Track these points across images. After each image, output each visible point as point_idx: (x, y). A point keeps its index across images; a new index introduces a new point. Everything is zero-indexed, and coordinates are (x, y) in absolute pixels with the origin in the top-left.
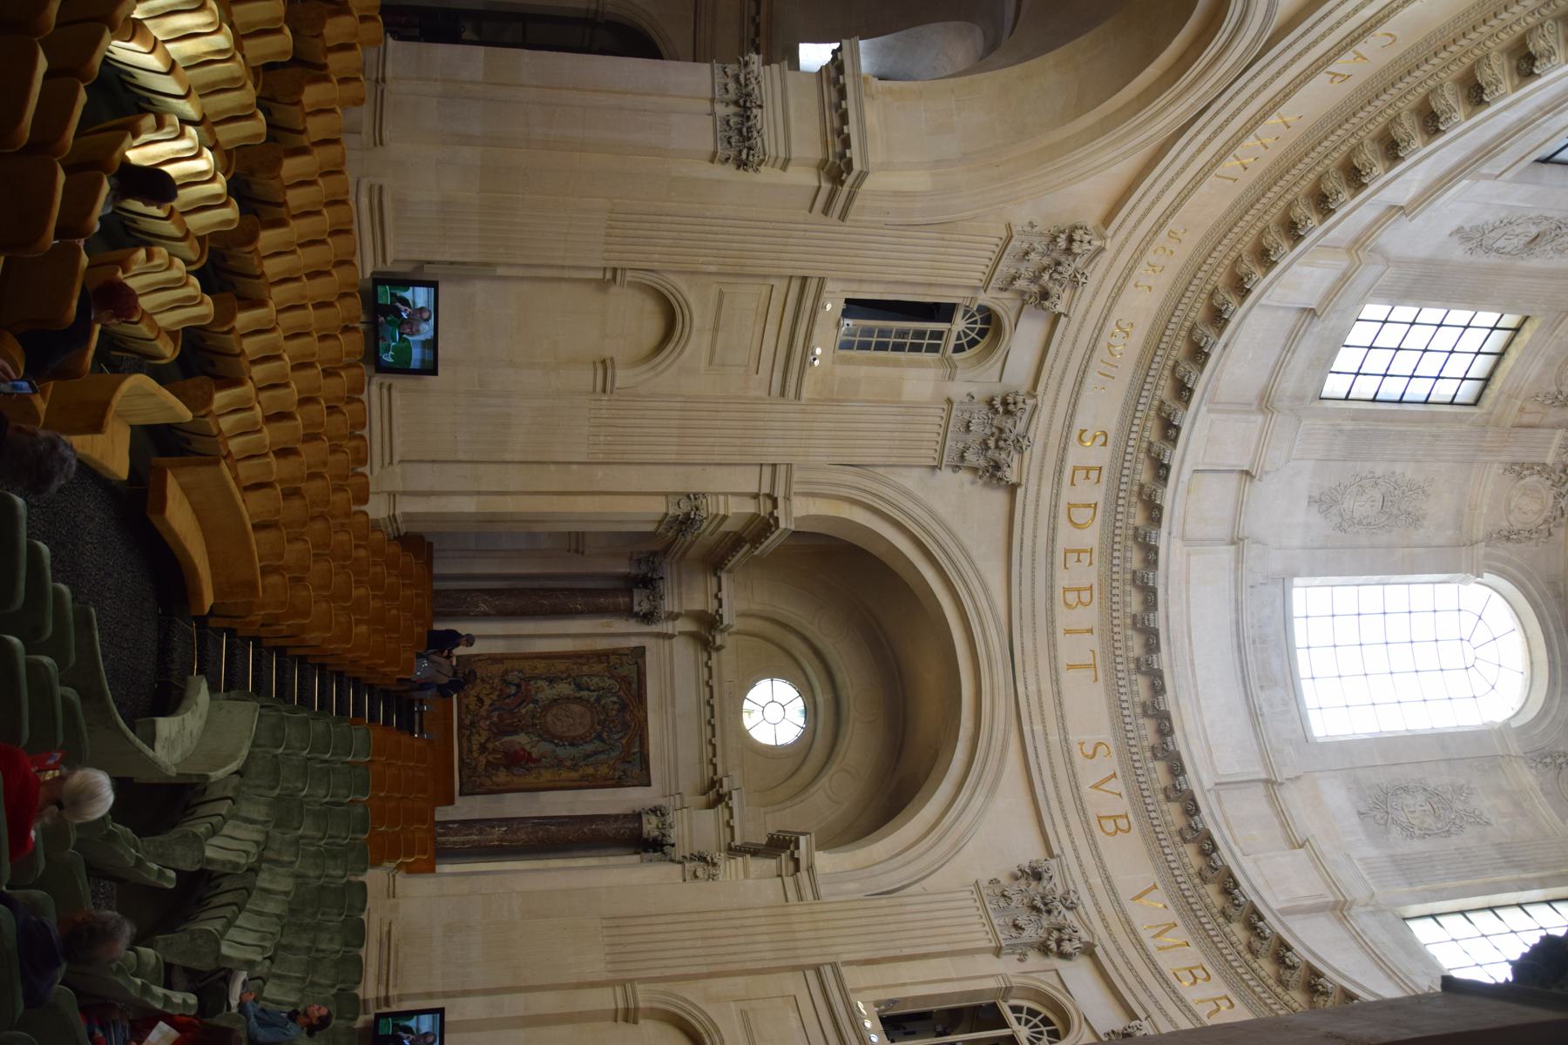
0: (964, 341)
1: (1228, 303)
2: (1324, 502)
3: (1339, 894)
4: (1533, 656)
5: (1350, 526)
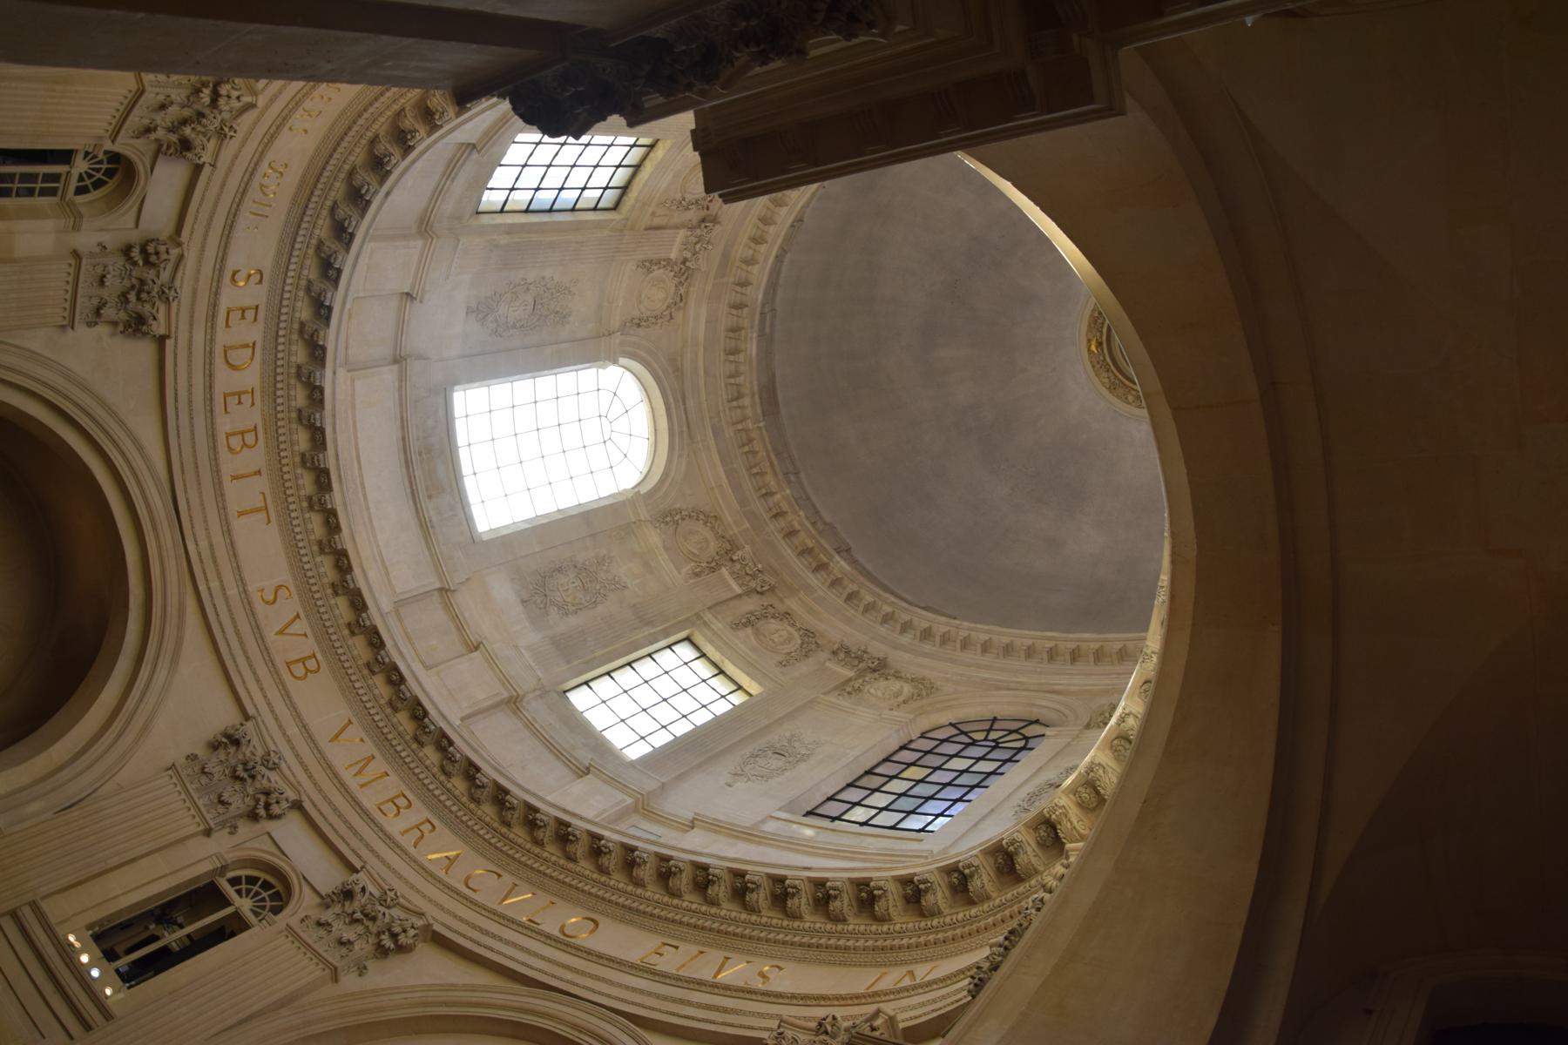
0: (88, 182)
1: (391, 155)
2: (480, 311)
3: (512, 690)
4: (657, 424)
5: (505, 330)
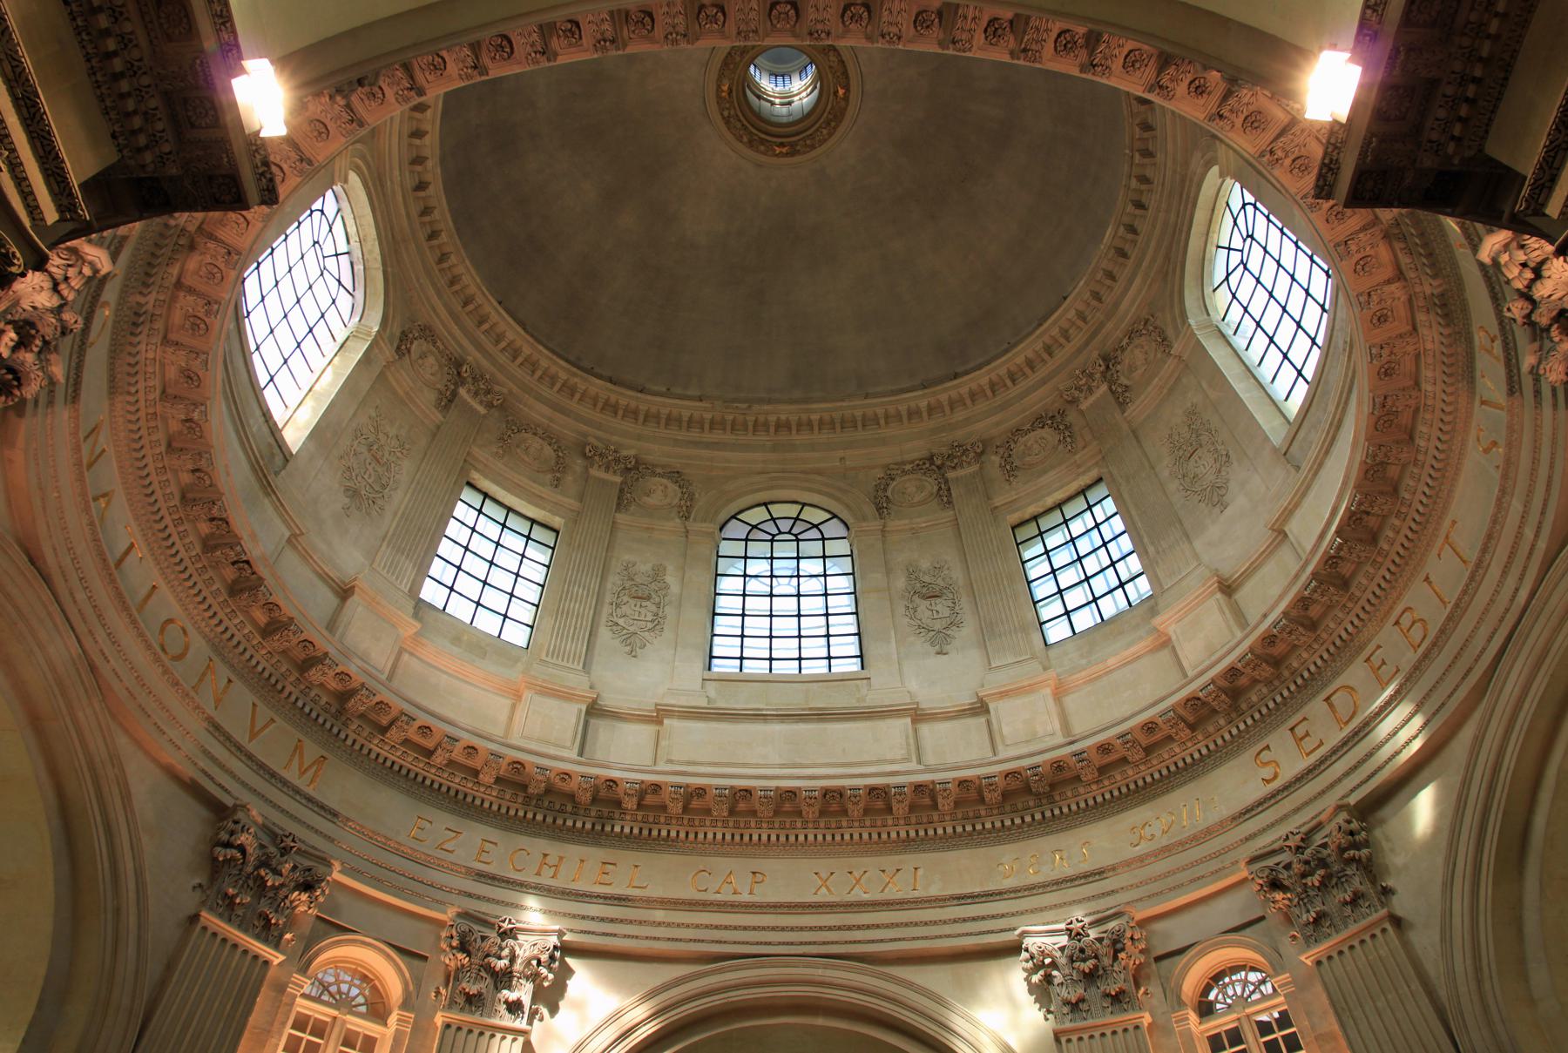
4: (1209, 217)
